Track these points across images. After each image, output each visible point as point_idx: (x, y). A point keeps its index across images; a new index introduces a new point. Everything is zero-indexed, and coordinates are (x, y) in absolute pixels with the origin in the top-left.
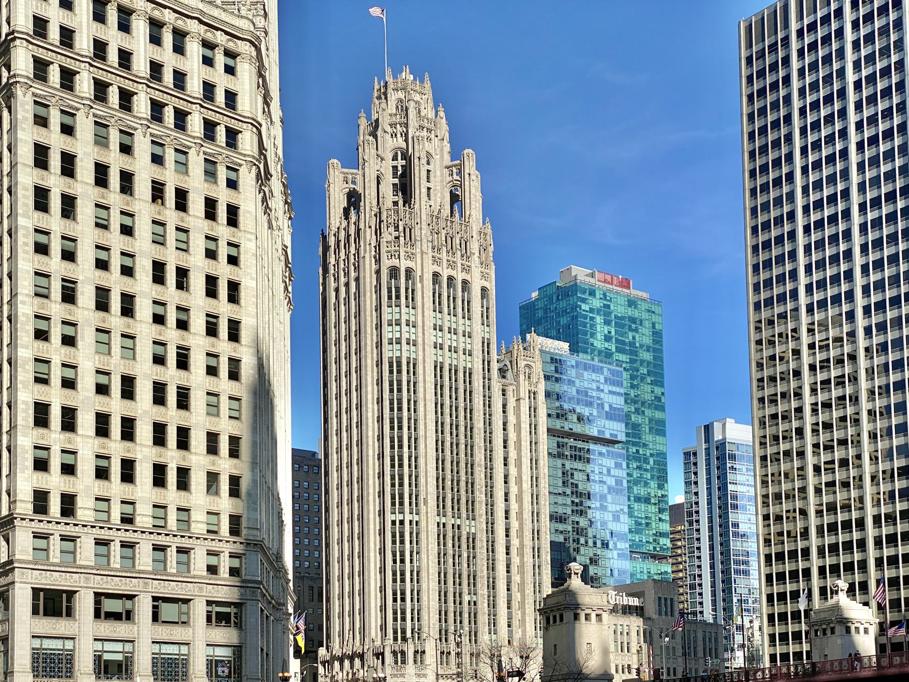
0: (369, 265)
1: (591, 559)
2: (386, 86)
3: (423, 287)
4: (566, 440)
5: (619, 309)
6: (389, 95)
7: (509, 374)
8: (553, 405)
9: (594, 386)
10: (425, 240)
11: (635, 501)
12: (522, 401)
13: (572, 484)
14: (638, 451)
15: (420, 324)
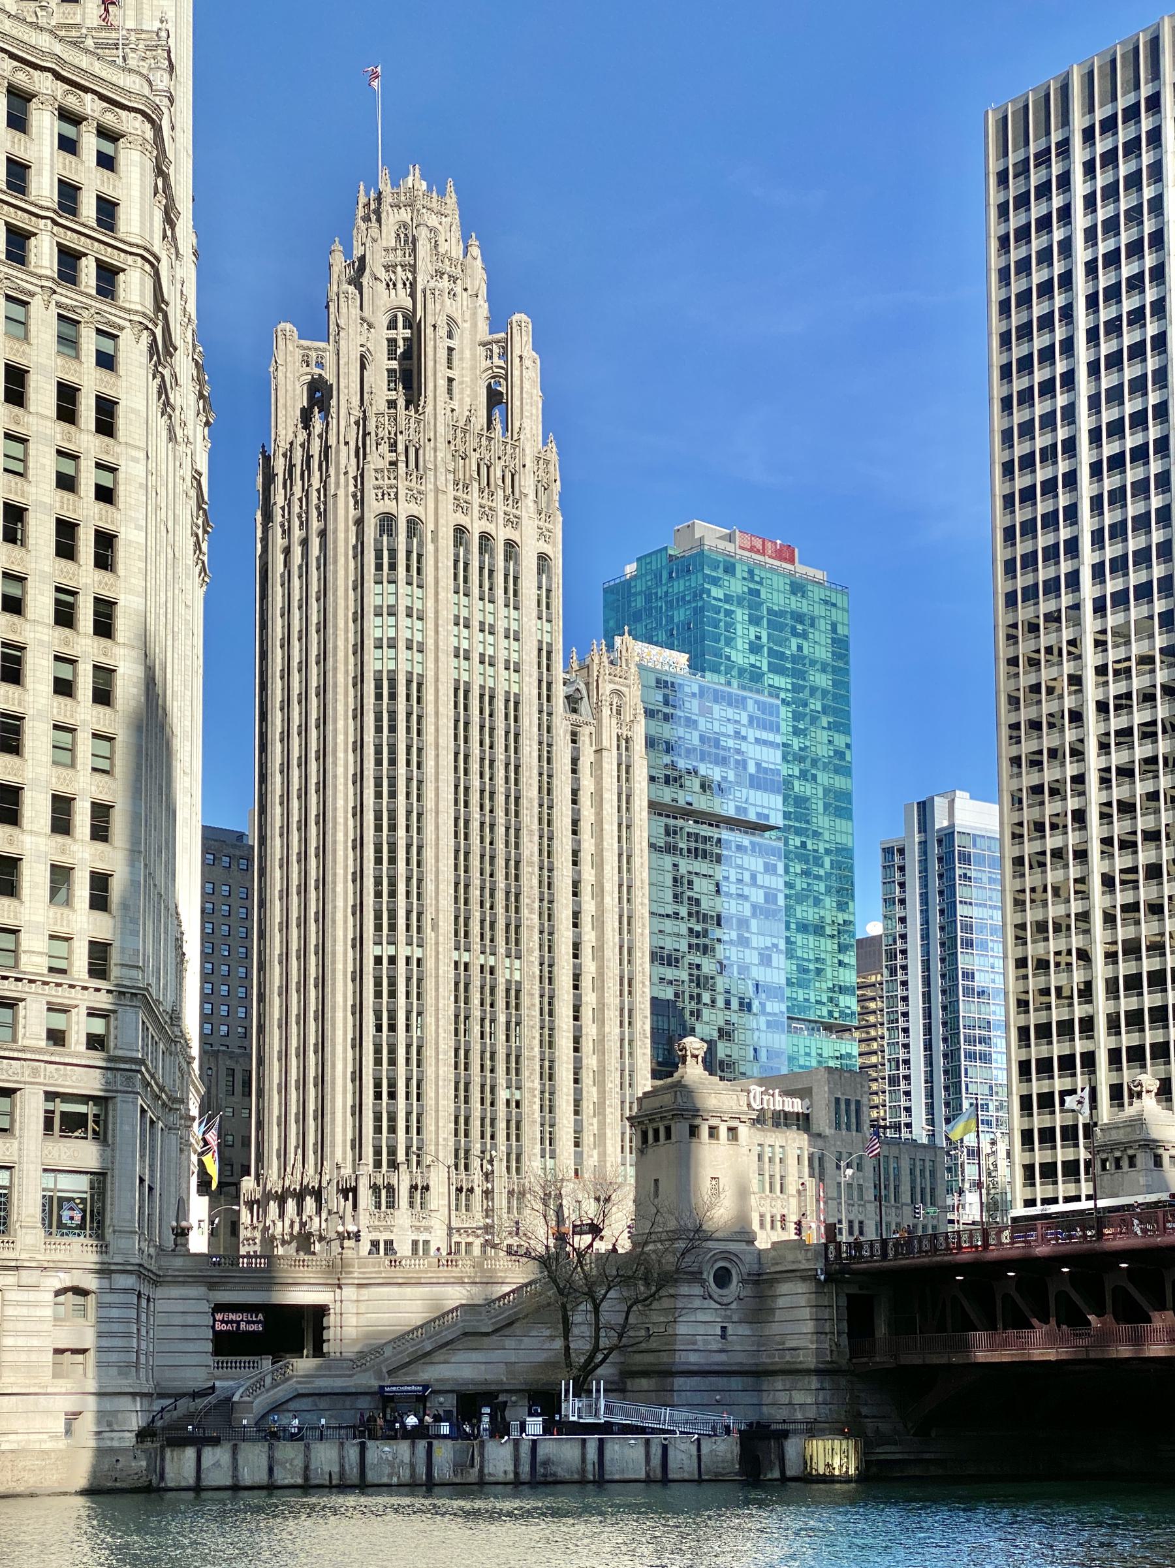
0: (343, 511)
1: (720, 1030)
2: (379, 199)
3: (436, 550)
4: (680, 822)
5: (777, 598)
6: (384, 215)
7: (584, 706)
8: (659, 761)
9: (730, 729)
10: (441, 470)
11: (798, 930)
12: (605, 753)
13: (690, 898)
14: (804, 844)
15: (430, 614)
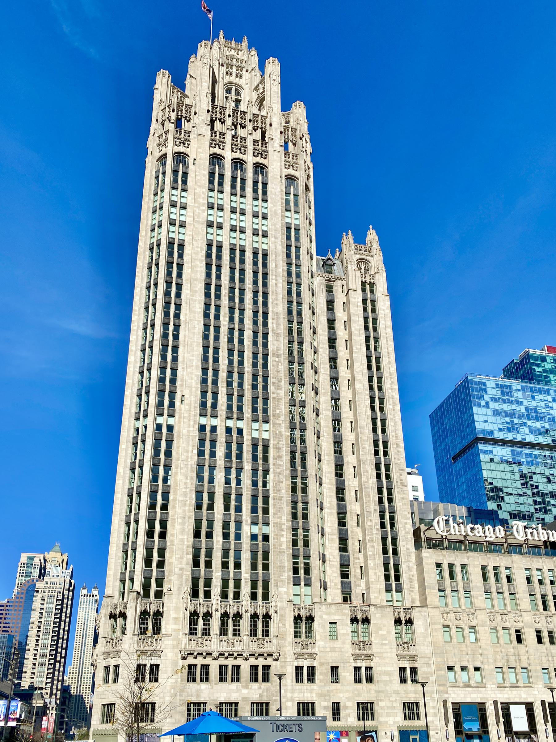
9: (543, 404)
13: (532, 485)
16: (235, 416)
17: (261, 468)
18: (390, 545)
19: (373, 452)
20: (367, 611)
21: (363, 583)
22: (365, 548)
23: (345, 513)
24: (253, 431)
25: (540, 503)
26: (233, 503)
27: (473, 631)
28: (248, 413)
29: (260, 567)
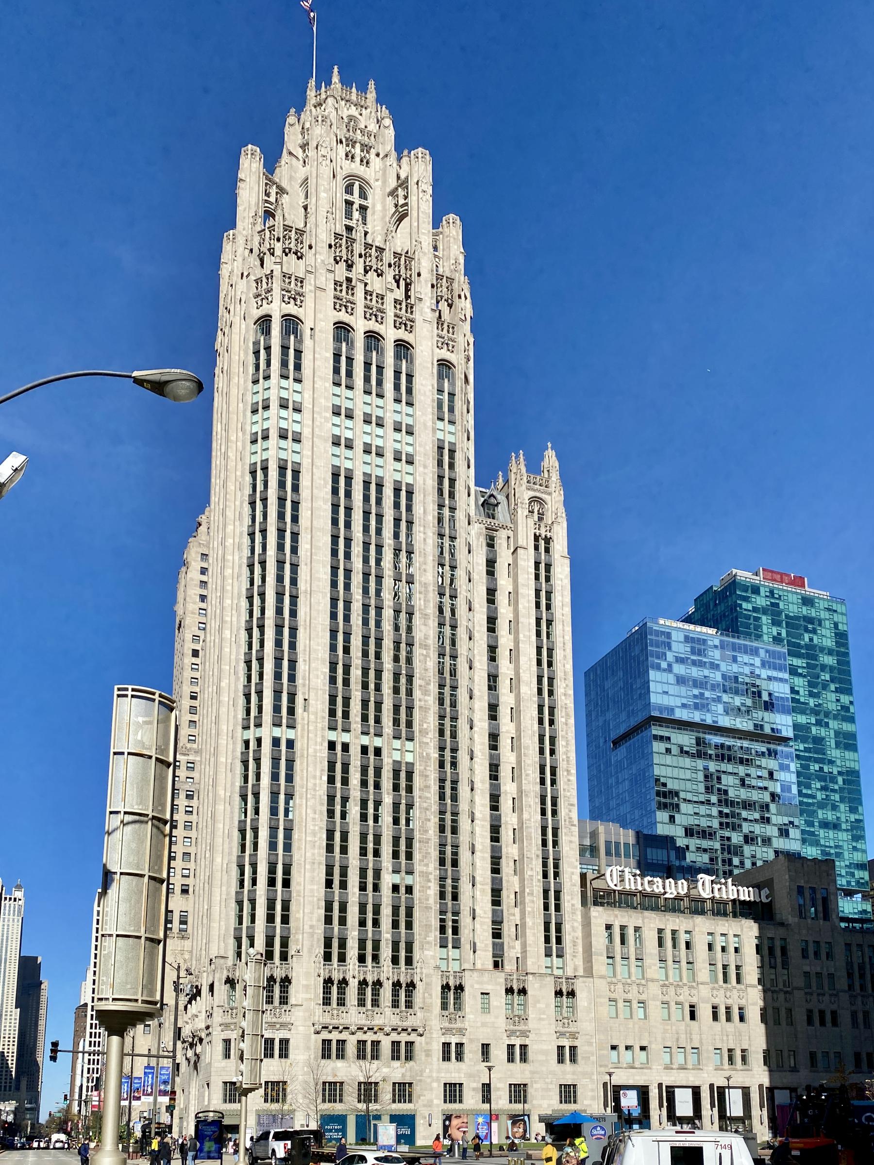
11: (820, 827)
13: (719, 790)
16: (372, 731)
17: (403, 801)
18: (552, 899)
19: (538, 780)
20: (524, 981)
21: (518, 944)
22: (523, 903)
23: (500, 858)
24: (394, 751)
25: (727, 815)
26: (370, 846)
27: (642, 1005)
28: (388, 727)
29: (403, 925)
